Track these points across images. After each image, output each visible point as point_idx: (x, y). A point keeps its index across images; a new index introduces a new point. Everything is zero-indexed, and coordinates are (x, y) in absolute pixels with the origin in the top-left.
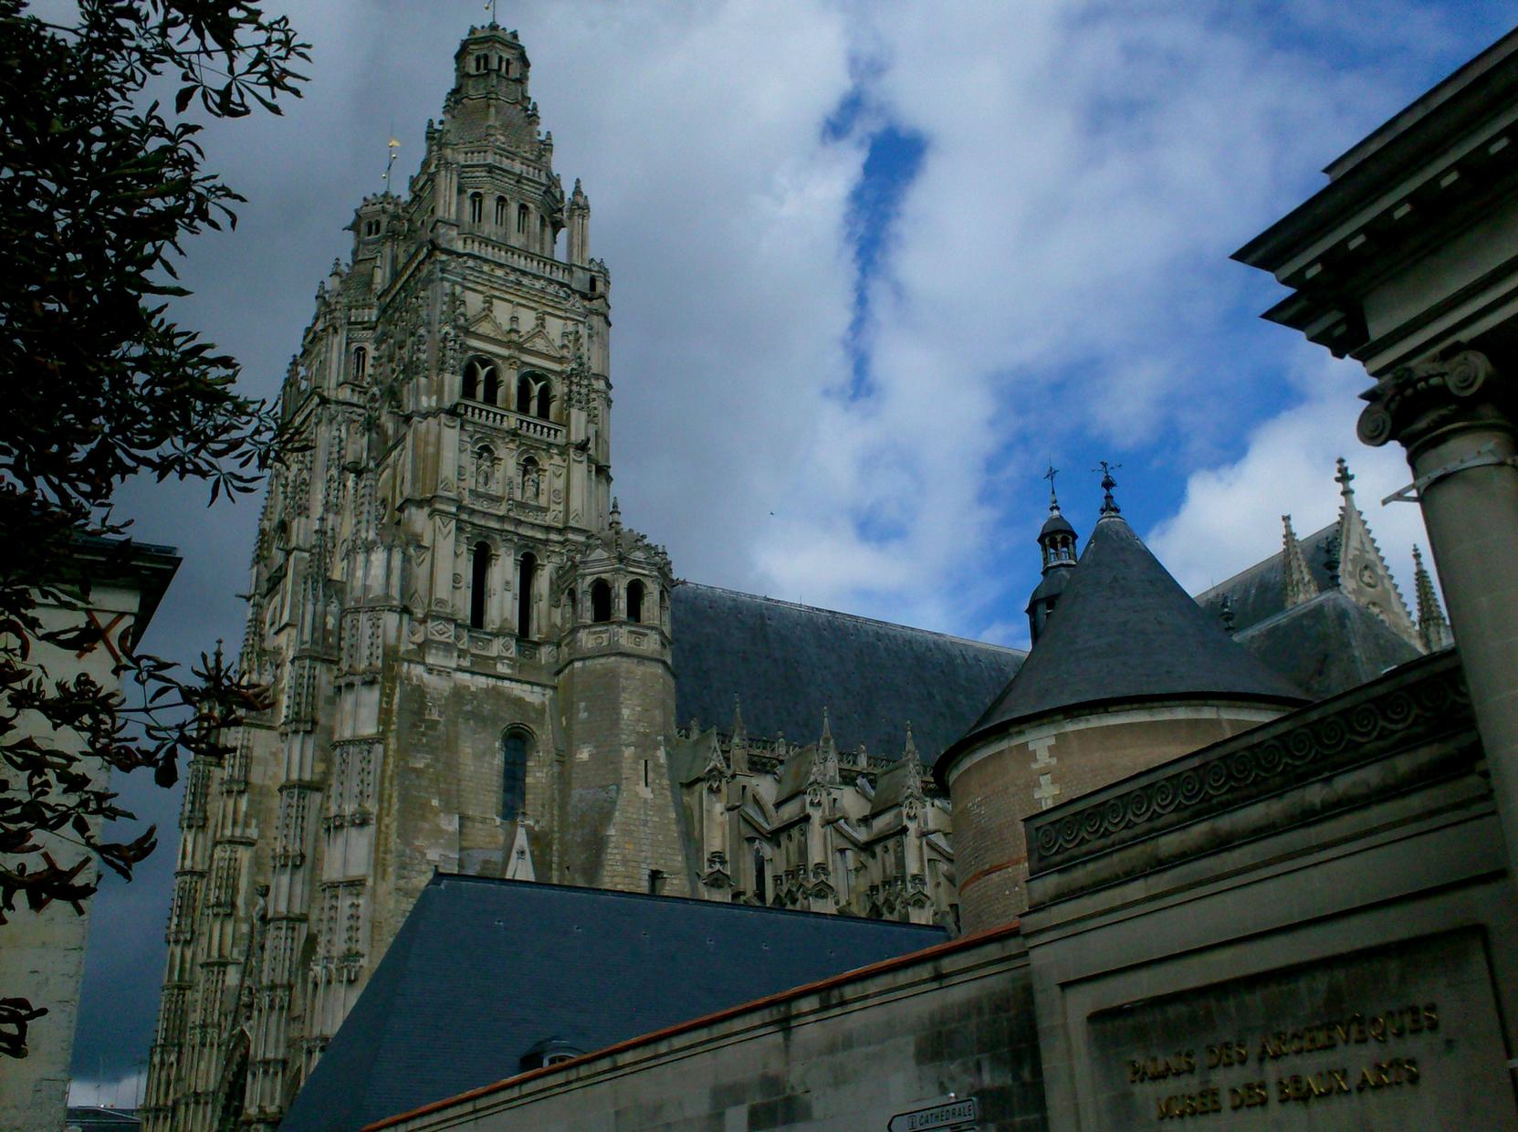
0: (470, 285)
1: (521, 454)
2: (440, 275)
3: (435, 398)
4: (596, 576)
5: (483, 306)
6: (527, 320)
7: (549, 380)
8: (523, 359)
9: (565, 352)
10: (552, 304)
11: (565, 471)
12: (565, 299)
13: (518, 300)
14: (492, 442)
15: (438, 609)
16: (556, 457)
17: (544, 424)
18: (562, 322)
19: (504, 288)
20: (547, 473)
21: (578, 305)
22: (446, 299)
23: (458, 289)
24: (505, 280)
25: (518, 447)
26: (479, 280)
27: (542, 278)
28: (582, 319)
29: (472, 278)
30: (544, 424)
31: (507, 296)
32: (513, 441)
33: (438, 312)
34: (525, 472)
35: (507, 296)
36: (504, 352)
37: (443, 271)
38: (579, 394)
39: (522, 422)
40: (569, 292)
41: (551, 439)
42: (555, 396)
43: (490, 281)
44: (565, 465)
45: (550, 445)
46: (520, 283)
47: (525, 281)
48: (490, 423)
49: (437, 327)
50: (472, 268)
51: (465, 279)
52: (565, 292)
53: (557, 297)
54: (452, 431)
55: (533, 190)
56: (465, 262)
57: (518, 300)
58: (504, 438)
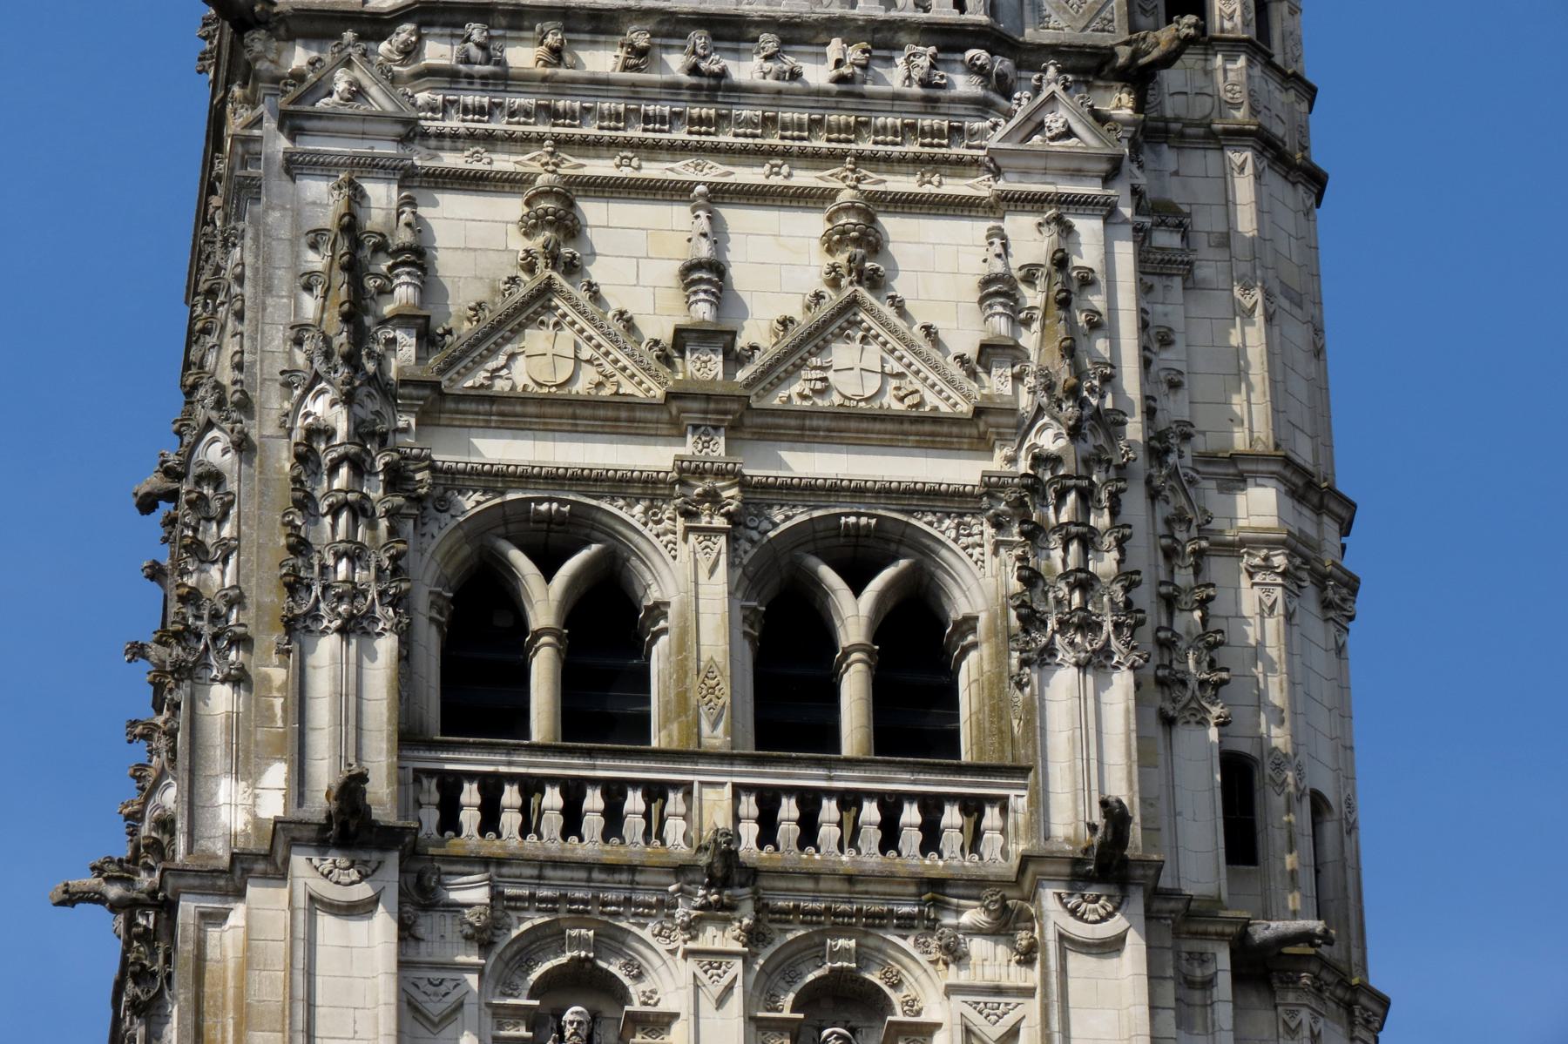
0: (452, 160)
1: (763, 989)
2: (283, 143)
3: (277, 774)
5: (519, 244)
7: (923, 548)
8: (754, 472)
9: (998, 383)
10: (913, 148)
11: (1033, 1007)
12: (982, 107)
13: (714, 172)
14: (610, 940)
16: (978, 947)
18: (975, 230)
19: (636, 132)
21: (1055, 121)
22: (316, 261)
23: (381, 195)
24: (634, 91)
25: (754, 937)
26: (499, 125)
28: (1092, 189)
29: (454, 123)
31: (654, 170)
32: (718, 912)
33: (278, 338)
35: (654, 170)
36: (655, 457)
37: (292, 124)
38: (1085, 582)
39: (768, 801)
40: (1002, 64)
41: (952, 856)
42: (969, 623)
43: (553, 114)
44: (1032, 977)
45: (936, 891)
46: (717, 87)
47: (747, 70)
48: (591, 843)
49: (273, 403)
50: (448, 76)
51: (411, 133)
52: (973, 69)
53: (930, 104)
54: (357, 927)
56: (410, 52)
57: (714, 172)
58: (665, 906)
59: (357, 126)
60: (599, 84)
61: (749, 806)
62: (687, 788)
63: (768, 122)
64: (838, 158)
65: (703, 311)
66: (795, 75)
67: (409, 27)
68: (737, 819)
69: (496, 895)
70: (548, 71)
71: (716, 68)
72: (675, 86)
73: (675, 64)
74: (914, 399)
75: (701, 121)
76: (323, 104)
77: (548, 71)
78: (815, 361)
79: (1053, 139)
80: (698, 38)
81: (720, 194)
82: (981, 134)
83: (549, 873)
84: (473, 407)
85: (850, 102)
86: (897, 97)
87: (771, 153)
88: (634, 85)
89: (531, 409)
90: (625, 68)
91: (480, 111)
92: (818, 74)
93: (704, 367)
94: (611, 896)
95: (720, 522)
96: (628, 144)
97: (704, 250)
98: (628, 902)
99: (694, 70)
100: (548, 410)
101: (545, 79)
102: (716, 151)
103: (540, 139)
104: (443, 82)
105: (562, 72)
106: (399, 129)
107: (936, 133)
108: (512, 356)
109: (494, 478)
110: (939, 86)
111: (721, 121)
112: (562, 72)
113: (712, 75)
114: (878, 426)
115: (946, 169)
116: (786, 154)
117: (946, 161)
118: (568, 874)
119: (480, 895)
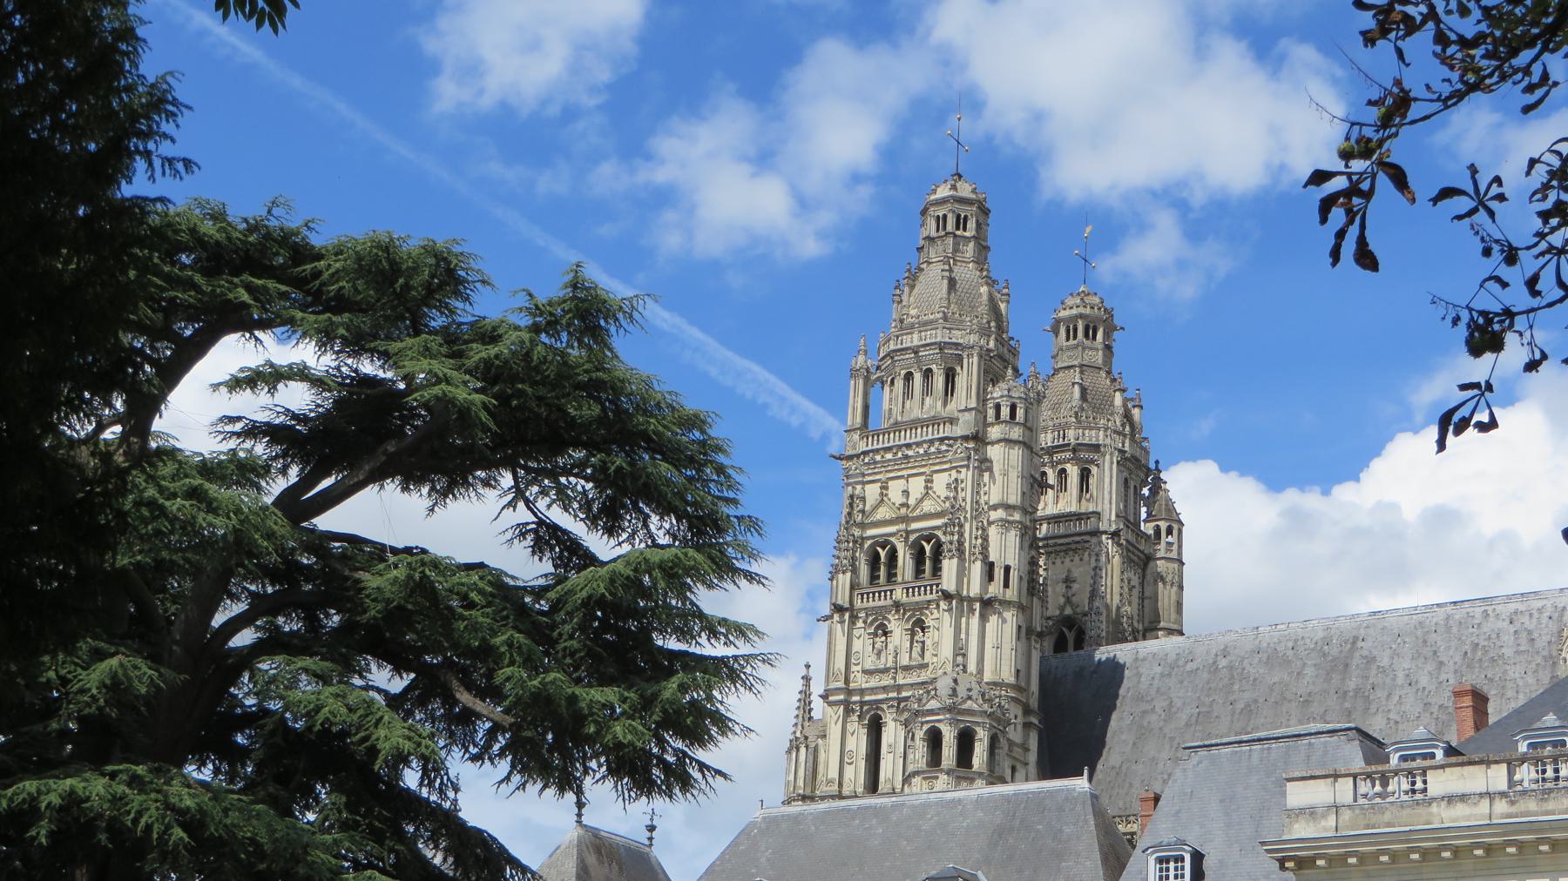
4: (929, 725)
6: (917, 486)
10: (938, 461)
13: (904, 473)
15: (828, 788)
17: (879, 589)
18: (947, 473)
20: (931, 629)
24: (895, 460)
27: (925, 441)
30: (879, 589)
34: (913, 634)
39: (908, 589)
45: (929, 602)
46: (906, 457)
50: (868, 464)
51: (863, 475)
53: (940, 452)
55: (931, 352)
56: (863, 460)
65: (905, 500)
73: (900, 455)
80: (904, 449)
81: (909, 476)
92: (921, 451)
93: (903, 511)
97: (905, 488)
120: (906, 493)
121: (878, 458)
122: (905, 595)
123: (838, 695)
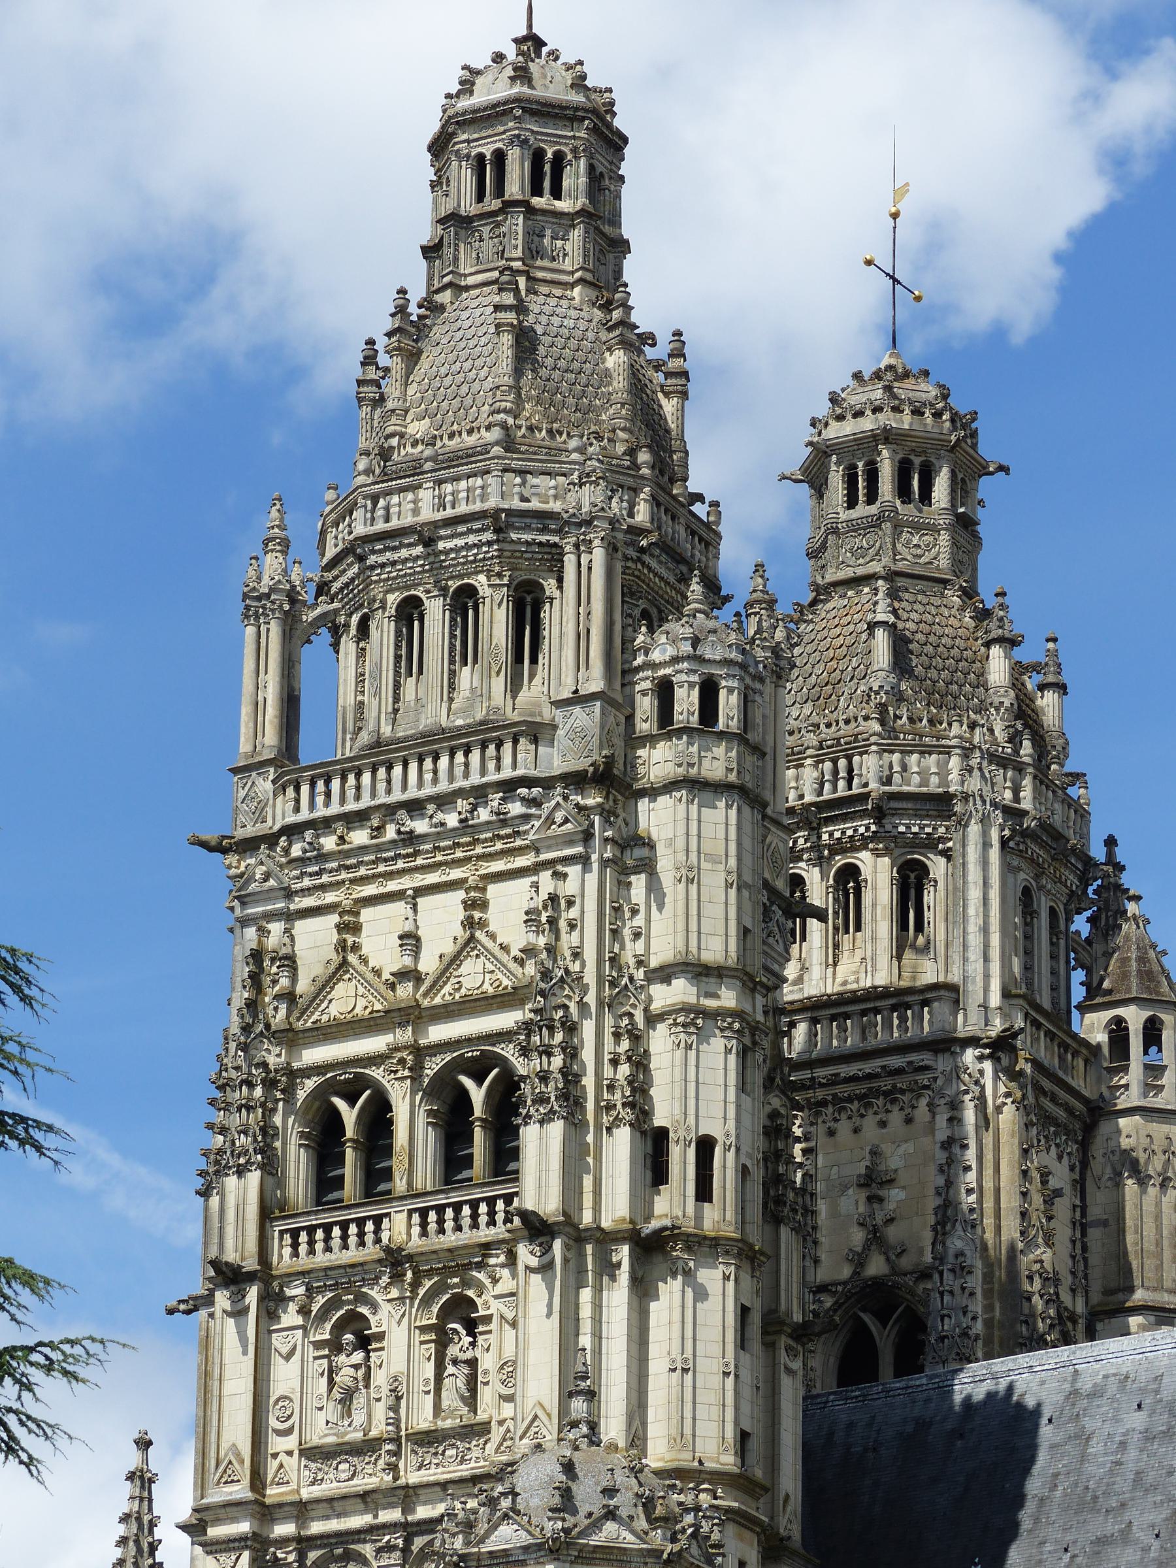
24: (379, 848)
46: (410, 838)
50: (302, 861)
51: (289, 894)
53: (504, 823)
56: (287, 851)
59: (266, 896)
60: (363, 849)
61: (416, 1218)
62: (388, 1215)
63: (437, 849)
64: (467, 860)
65: (408, 961)
66: (442, 824)
67: (283, 838)
68: (410, 1226)
69: (309, 1289)
70: (340, 848)
71: (407, 829)
72: (393, 842)
73: (391, 832)
74: (497, 983)
75: (408, 855)
76: (253, 887)
77: (340, 848)
78: (456, 974)
79: (559, 826)
82: (526, 832)
83: (329, 1273)
84: (310, 1034)
85: (469, 830)
86: (488, 823)
87: (439, 865)
88: (377, 845)
89: (334, 1030)
90: (373, 838)
91: (316, 874)
92: (452, 820)
93: (405, 991)
94: (357, 1278)
95: (406, 1073)
96: (380, 875)
97: (408, 927)
98: (363, 1280)
99: (399, 832)
100: (341, 1029)
101: (340, 852)
102: (417, 869)
103: (343, 882)
104: (299, 863)
105: (346, 847)
106: (283, 892)
107: (508, 836)
108: (330, 1001)
109: (318, 1069)
110: (504, 814)
111: (416, 854)
112: (346, 847)
113: (407, 833)
114: (478, 1004)
115: (516, 853)
116: (446, 863)
117: (515, 849)
118: (337, 1272)
119: (301, 1290)
120: (411, 940)
121: (329, 843)
122: (416, 1230)
123: (234, 1520)
